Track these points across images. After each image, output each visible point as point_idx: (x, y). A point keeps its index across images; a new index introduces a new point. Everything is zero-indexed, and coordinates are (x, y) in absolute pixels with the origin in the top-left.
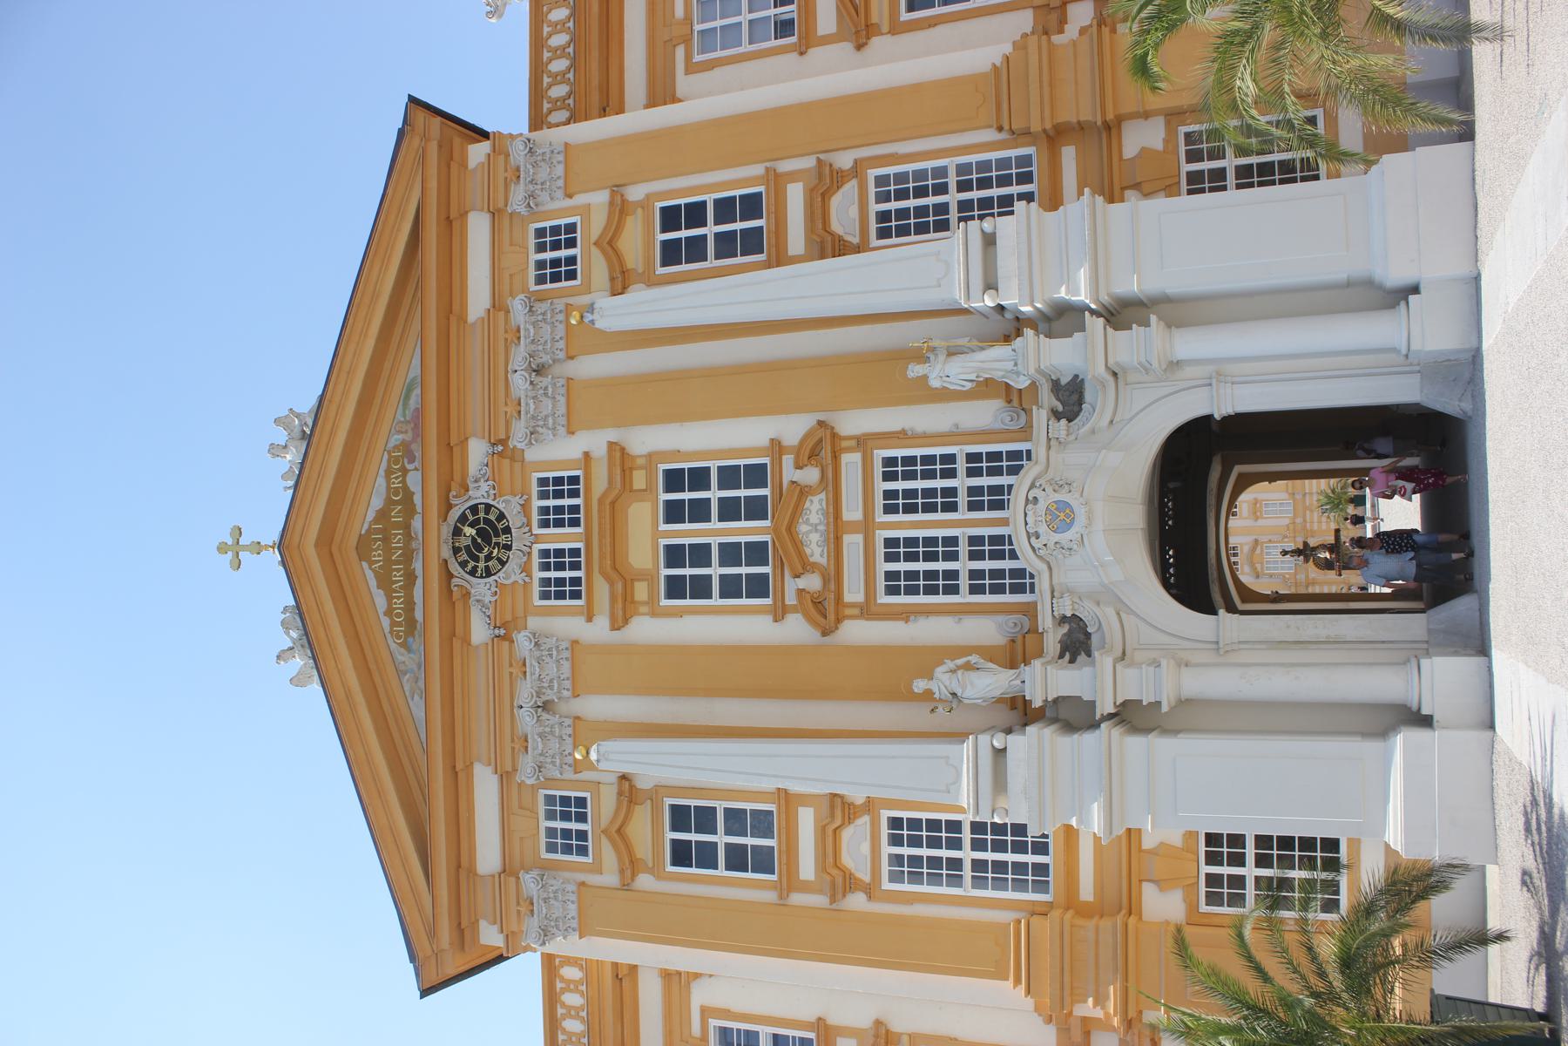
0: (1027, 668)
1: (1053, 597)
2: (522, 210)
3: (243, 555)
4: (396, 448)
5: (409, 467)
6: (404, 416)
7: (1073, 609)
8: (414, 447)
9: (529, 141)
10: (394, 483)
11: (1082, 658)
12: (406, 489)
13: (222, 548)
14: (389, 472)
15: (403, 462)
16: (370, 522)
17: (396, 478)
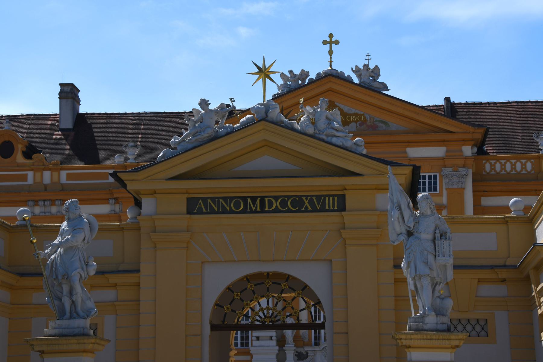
0: (293, 345)
1: (313, 350)
2: (442, 173)
3: (328, 45)
4: (365, 118)
5: (358, 124)
6: (376, 121)
7: (310, 356)
8: (365, 125)
9: (466, 176)
10: (352, 117)
11: (296, 358)
12: (351, 122)
13: (331, 36)
14: (356, 114)
15: (359, 121)
16: (339, 107)
17: (354, 118)
